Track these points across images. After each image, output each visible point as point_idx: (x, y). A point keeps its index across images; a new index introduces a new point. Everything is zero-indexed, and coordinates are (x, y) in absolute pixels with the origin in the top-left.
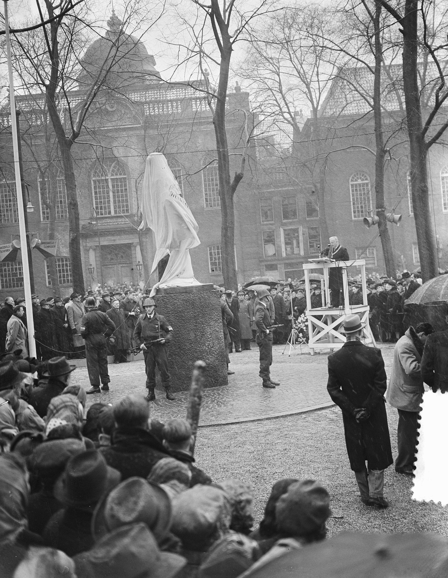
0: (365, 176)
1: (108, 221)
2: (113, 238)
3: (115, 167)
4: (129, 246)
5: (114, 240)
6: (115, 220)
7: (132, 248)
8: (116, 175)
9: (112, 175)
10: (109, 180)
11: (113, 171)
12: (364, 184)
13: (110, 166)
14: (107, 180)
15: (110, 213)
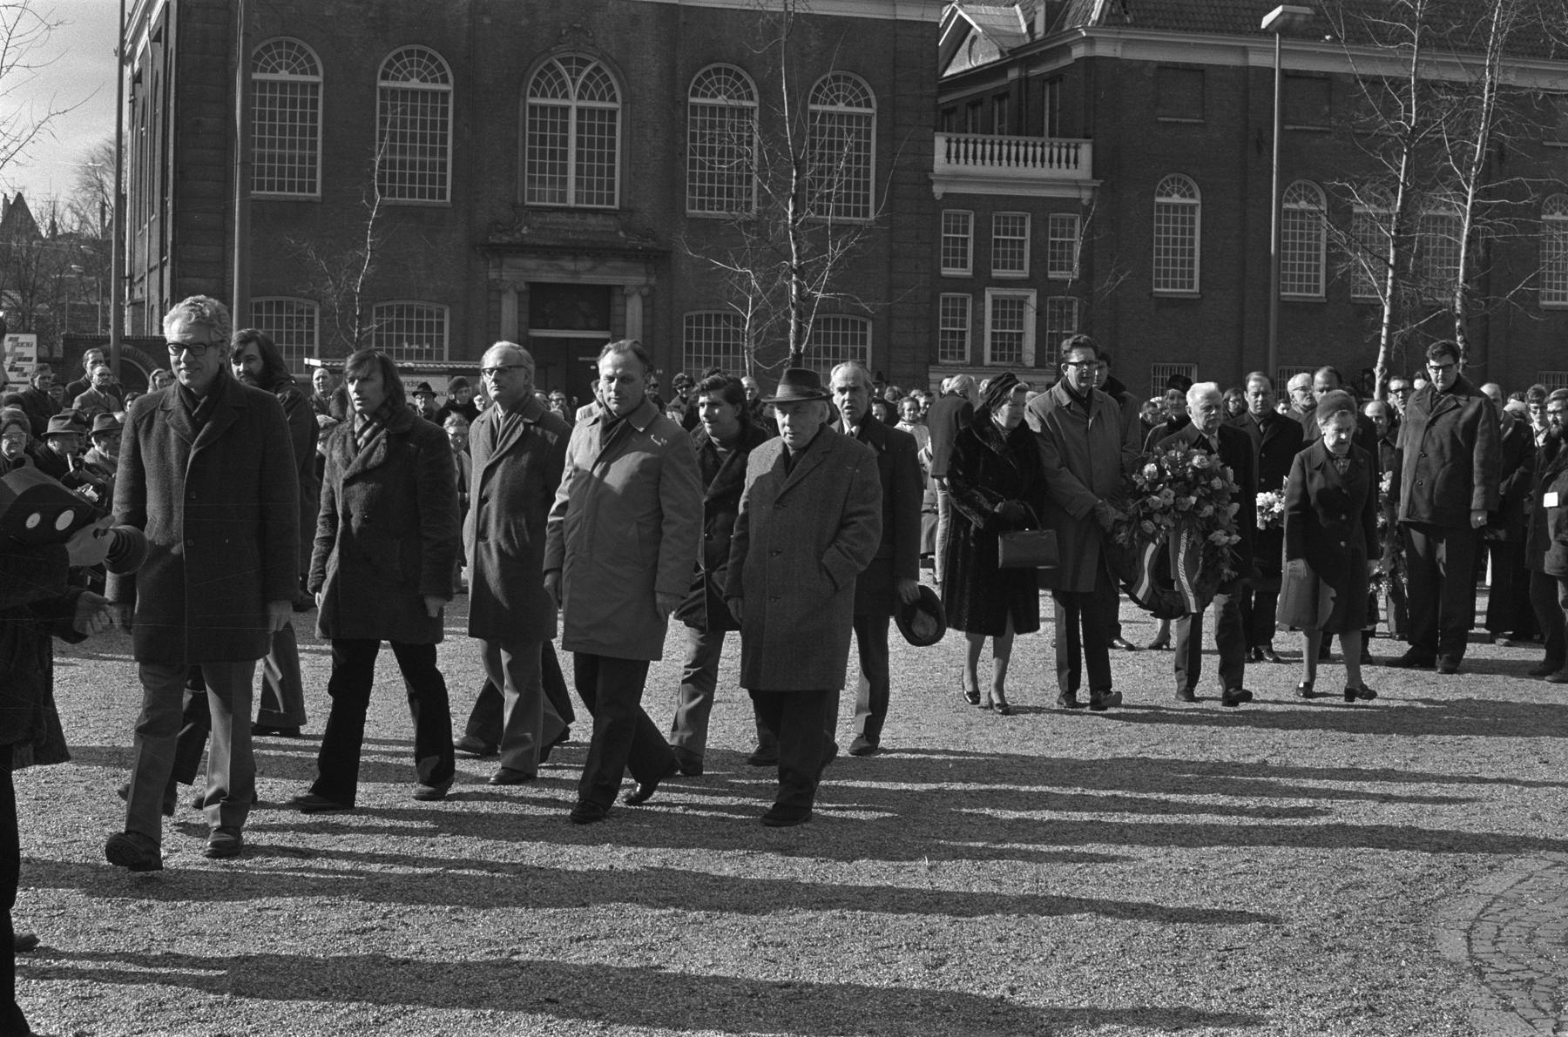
0: (1190, 188)
1: (563, 218)
2: (569, 265)
3: (589, 77)
4: (608, 290)
5: (576, 273)
6: (577, 218)
7: (617, 300)
8: (592, 98)
9: (580, 97)
10: (573, 115)
11: (584, 86)
12: (1184, 206)
13: (578, 72)
14: (566, 110)
15: (563, 198)
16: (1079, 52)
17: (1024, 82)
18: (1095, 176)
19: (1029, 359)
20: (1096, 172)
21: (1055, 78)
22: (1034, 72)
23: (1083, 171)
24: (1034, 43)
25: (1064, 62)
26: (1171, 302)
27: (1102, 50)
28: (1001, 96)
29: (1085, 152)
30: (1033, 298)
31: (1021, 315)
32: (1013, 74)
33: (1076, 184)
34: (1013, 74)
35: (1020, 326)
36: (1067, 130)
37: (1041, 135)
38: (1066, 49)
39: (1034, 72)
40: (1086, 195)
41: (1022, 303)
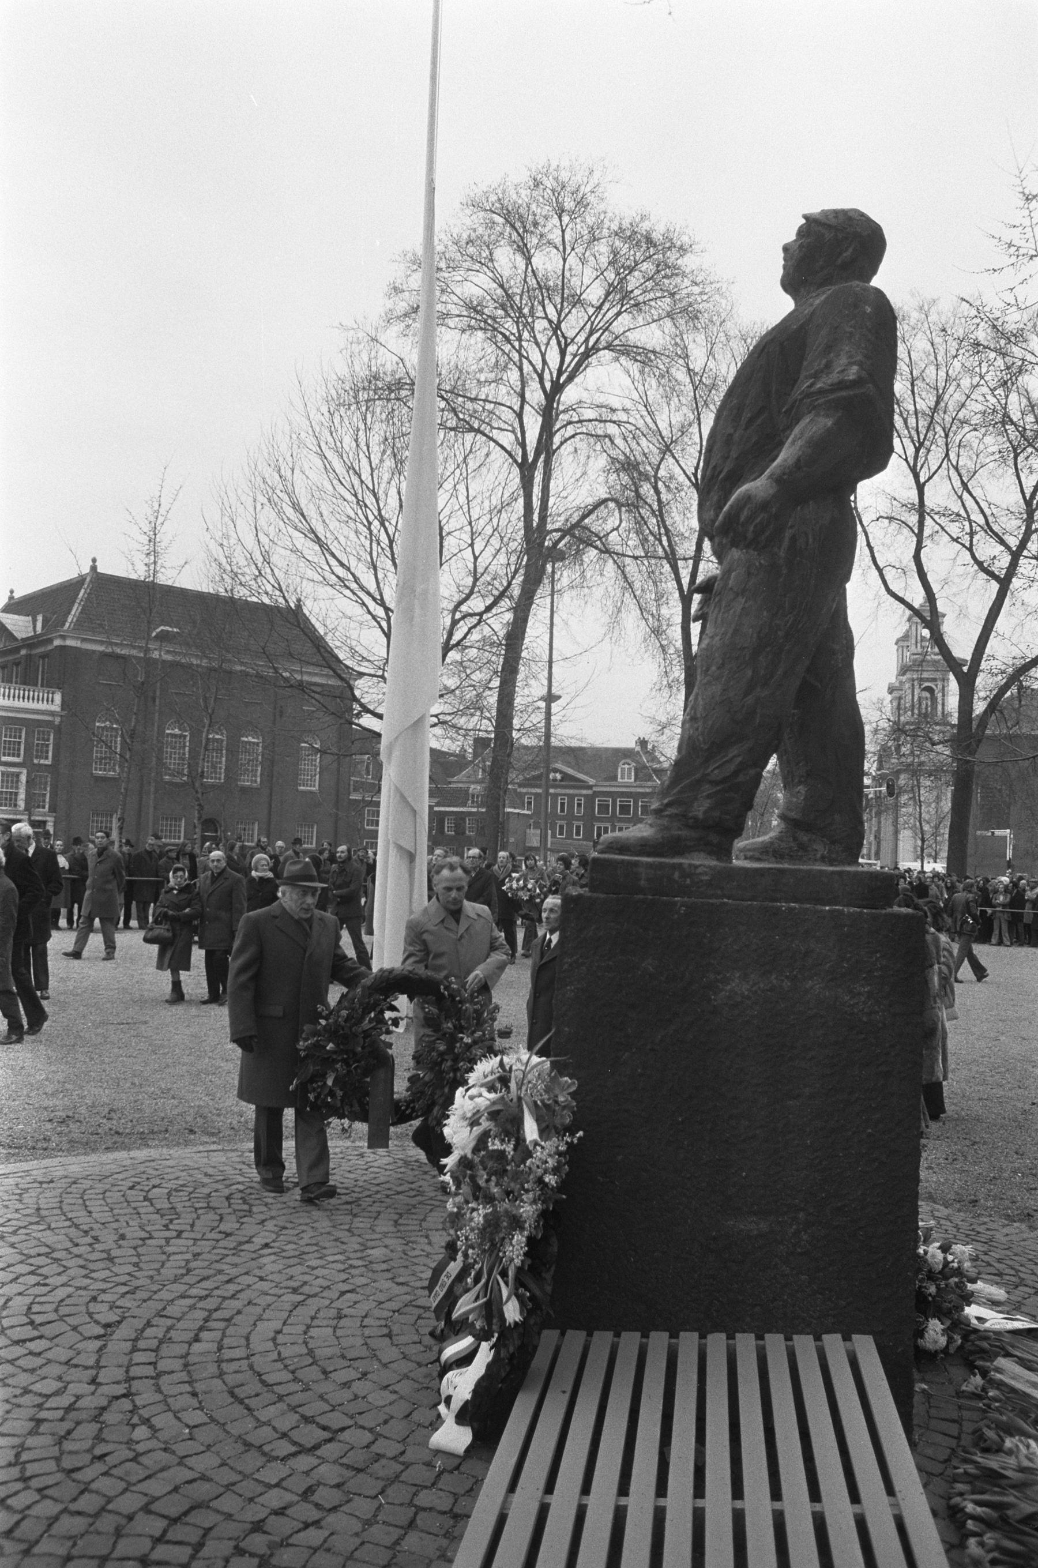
16: (57, 642)
17: (29, 657)
18: (62, 709)
19: (22, 804)
20: (64, 705)
21: (44, 656)
22: (34, 652)
23: (56, 706)
24: (36, 636)
25: (50, 647)
26: (104, 779)
27: (69, 643)
28: (17, 664)
29: (58, 697)
30: (25, 771)
31: (17, 781)
32: (23, 652)
33: (52, 713)
34: (23, 652)
35: (17, 788)
36: (50, 684)
37: (36, 685)
38: (50, 641)
39: (34, 652)
40: (57, 720)
41: (18, 775)
